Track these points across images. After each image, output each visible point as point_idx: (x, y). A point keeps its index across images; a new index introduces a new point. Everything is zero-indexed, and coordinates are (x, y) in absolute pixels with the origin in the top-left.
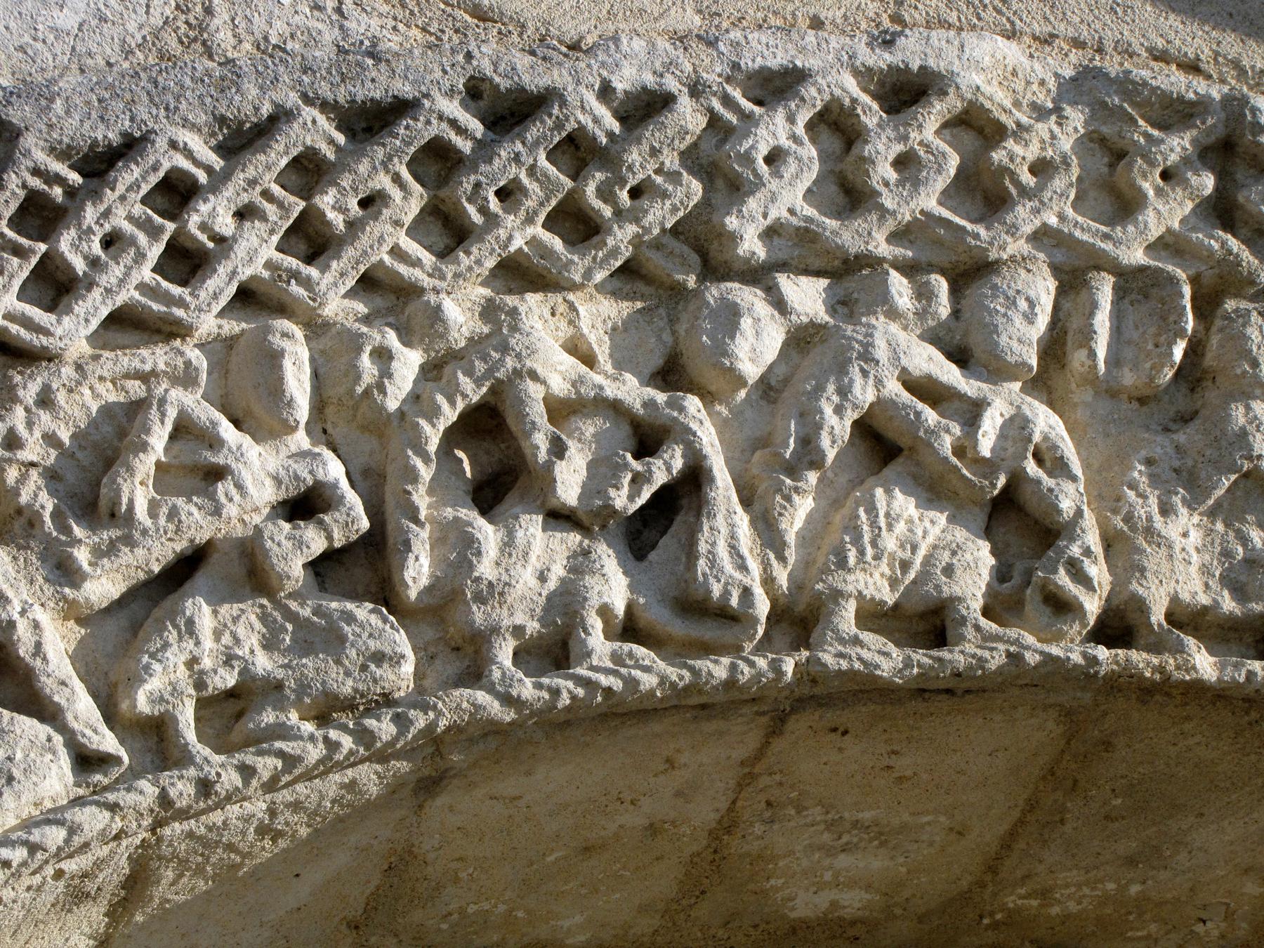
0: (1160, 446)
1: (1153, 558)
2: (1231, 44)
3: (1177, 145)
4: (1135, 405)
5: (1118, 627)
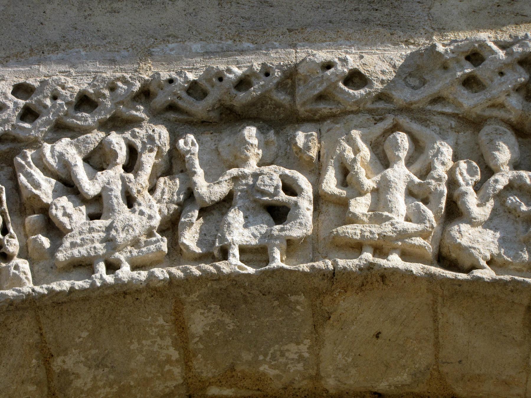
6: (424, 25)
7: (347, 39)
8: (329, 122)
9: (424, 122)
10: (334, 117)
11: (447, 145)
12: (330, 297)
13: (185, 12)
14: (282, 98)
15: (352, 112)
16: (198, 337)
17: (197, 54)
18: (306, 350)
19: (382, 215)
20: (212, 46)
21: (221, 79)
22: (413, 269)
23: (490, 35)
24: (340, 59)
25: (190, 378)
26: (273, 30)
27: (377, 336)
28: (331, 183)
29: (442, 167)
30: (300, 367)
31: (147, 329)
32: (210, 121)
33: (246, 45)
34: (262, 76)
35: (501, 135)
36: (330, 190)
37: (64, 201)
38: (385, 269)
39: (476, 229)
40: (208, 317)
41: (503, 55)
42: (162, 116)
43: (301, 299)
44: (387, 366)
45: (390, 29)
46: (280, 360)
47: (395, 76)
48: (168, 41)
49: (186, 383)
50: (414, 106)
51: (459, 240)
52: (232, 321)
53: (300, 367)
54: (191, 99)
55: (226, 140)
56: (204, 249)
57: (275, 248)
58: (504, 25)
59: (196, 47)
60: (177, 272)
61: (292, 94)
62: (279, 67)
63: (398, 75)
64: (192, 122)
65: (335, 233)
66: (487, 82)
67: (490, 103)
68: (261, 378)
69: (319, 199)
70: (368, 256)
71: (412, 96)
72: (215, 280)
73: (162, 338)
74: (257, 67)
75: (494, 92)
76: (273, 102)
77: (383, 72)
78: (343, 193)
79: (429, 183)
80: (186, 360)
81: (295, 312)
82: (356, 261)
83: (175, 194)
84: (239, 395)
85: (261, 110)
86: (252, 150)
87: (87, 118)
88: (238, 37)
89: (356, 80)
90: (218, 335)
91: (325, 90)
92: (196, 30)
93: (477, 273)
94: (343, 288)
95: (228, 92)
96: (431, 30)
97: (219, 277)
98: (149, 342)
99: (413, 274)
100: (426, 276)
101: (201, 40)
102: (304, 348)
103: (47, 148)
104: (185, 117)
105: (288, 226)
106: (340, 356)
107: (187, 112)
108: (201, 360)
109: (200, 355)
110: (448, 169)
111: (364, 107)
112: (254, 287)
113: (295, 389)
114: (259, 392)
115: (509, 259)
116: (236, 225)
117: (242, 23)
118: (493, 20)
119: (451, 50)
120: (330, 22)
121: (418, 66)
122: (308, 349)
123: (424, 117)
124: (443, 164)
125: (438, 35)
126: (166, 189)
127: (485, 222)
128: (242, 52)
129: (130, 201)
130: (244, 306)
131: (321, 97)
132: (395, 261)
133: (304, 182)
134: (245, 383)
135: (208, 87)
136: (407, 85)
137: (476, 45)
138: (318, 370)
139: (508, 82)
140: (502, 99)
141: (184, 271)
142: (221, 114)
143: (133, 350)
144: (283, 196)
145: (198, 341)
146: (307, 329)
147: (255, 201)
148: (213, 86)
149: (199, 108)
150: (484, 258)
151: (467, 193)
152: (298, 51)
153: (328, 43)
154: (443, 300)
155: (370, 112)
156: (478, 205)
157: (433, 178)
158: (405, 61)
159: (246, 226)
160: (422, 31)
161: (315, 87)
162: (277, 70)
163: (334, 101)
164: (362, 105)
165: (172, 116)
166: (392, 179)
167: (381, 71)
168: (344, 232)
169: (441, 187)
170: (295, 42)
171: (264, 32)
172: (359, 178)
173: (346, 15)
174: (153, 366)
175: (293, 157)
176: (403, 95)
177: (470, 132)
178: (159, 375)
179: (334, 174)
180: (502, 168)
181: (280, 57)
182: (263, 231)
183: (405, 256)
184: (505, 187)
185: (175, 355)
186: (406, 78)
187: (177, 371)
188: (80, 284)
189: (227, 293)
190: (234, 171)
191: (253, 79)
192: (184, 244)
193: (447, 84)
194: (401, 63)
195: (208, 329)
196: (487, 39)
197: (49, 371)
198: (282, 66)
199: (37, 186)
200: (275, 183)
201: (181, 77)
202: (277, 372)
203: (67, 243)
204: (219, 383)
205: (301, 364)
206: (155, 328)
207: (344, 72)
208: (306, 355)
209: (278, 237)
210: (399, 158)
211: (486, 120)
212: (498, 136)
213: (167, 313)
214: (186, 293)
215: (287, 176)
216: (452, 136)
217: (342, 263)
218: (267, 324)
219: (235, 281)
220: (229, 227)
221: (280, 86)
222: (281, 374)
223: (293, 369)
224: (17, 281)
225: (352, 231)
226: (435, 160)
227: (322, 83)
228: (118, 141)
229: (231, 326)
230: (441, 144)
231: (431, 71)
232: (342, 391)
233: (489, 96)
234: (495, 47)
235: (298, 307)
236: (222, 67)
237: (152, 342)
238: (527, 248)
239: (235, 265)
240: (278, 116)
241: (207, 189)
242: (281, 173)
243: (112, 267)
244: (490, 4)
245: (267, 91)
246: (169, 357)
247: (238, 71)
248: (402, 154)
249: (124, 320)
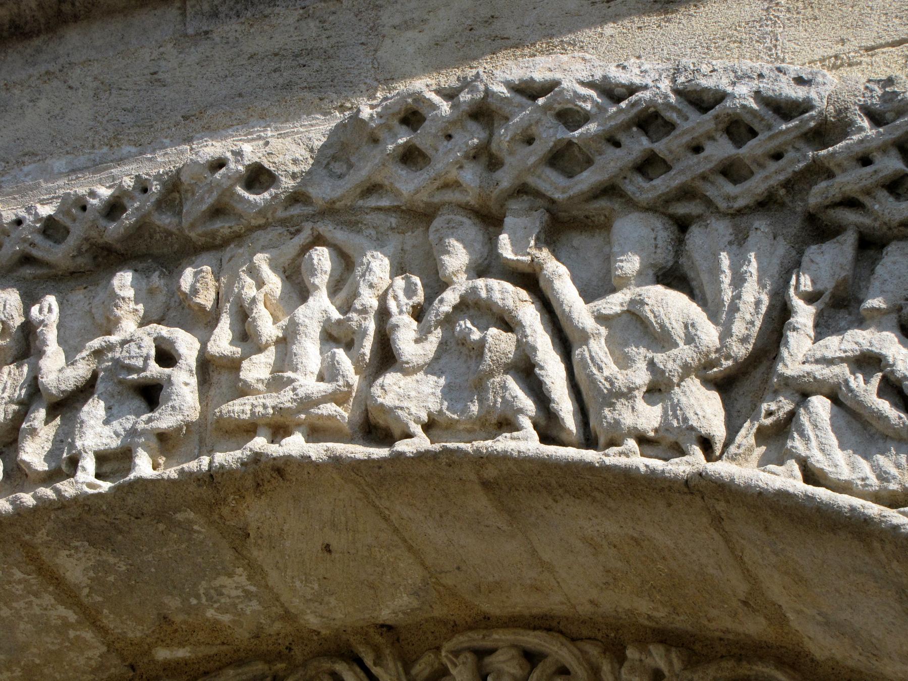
6: (366, 77)
7: (262, 117)
8: (232, 246)
9: (354, 226)
10: (237, 238)
11: (380, 255)
13: (49, 116)
14: (167, 221)
15: (260, 227)
17: (60, 175)
19: (282, 377)
20: (82, 160)
21: (84, 208)
22: (311, 454)
23: (429, 81)
24: (233, 152)
26: (162, 122)
28: (222, 341)
29: (370, 291)
30: (255, 605)
31: (7, 587)
33: (126, 149)
34: (137, 194)
35: (452, 229)
36: (218, 350)
38: (274, 459)
39: (415, 377)
41: (448, 109)
42: (15, 274)
44: (372, 586)
45: (320, 92)
47: (313, 165)
48: (23, 162)
50: (338, 205)
51: (380, 400)
53: (255, 605)
54: (48, 243)
56: (53, 464)
57: (140, 450)
58: (475, 59)
59: (59, 164)
60: (28, 499)
62: (158, 177)
63: (317, 162)
64: (56, 276)
65: (218, 414)
66: (430, 152)
67: (437, 184)
68: (215, 628)
69: (207, 367)
70: (259, 443)
71: (333, 190)
72: (59, 509)
74: (128, 182)
75: (439, 166)
77: (295, 161)
78: (237, 351)
79: (349, 319)
81: (196, 535)
82: (238, 453)
83: (18, 388)
84: (200, 655)
86: (125, 307)
88: (115, 140)
89: (264, 178)
91: (218, 201)
92: (61, 139)
93: (403, 446)
95: (94, 225)
96: (376, 83)
97: (62, 504)
99: (312, 462)
100: (330, 461)
101: (68, 153)
104: (44, 271)
105: (156, 414)
108: (112, 616)
109: (105, 611)
110: (380, 293)
111: (273, 217)
112: (117, 509)
113: (270, 635)
114: (225, 648)
115: (455, 417)
116: (92, 422)
117: (121, 120)
118: (461, 53)
119: (378, 114)
120: (240, 95)
121: (343, 143)
122: (248, 579)
123: (354, 218)
124: (371, 286)
125: (384, 89)
126: (9, 385)
127: (429, 365)
130: (120, 537)
131: (218, 211)
132: (295, 445)
134: (199, 637)
135: (67, 222)
136: (331, 174)
137: (410, 100)
138: (282, 605)
139: (457, 148)
140: (454, 174)
141: (12, 503)
142: (95, 258)
144: (154, 369)
146: (228, 555)
147: (121, 382)
148: (74, 220)
149: (58, 254)
150: (417, 421)
151: (398, 326)
152: (194, 146)
153: (235, 128)
154: (373, 489)
156: (417, 341)
157: (356, 311)
158: (328, 138)
159: (106, 422)
160: (363, 87)
161: (202, 199)
162: (155, 183)
164: (269, 215)
166: (301, 321)
167: (292, 160)
168: (229, 412)
169: (367, 322)
170: (191, 135)
171: (152, 126)
172: (256, 326)
173: (261, 82)
174: (51, 634)
176: (324, 191)
177: (421, 229)
179: (228, 326)
180: (455, 279)
181: (159, 164)
182: (128, 426)
183: (315, 433)
184: (455, 308)
186: (328, 164)
190: (97, 343)
191: (125, 201)
192: (24, 462)
193: (376, 164)
194: (321, 143)
196: (424, 89)
198: (162, 175)
200: (145, 351)
201: (30, 214)
207: (237, 171)
208: (253, 589)
209: (144, 432)
210: (316, 288)
211: (439, 209)
212: (450, 232)
214: (28, 533)
215: (163, 338)
216: (395, 241)
217: (220, 458)
219: (87, 505)
220: (81, 427)
221: (163, 205)
225: (240, 408)
226: (361, 283)
227: (210, 191)
230: (373, 256)
231: (357, 149)
232: (337, 630)
233: (432, 174)
234: (436, 99)
235: (196, 527)
236: (82, 191)
238: (478, 395)
239: (83, 483)
242: (155, 335)
244: (460, 29)
245: (144, 216)
246: (64, 619)
247: (105, 192)
248: (319, 280)
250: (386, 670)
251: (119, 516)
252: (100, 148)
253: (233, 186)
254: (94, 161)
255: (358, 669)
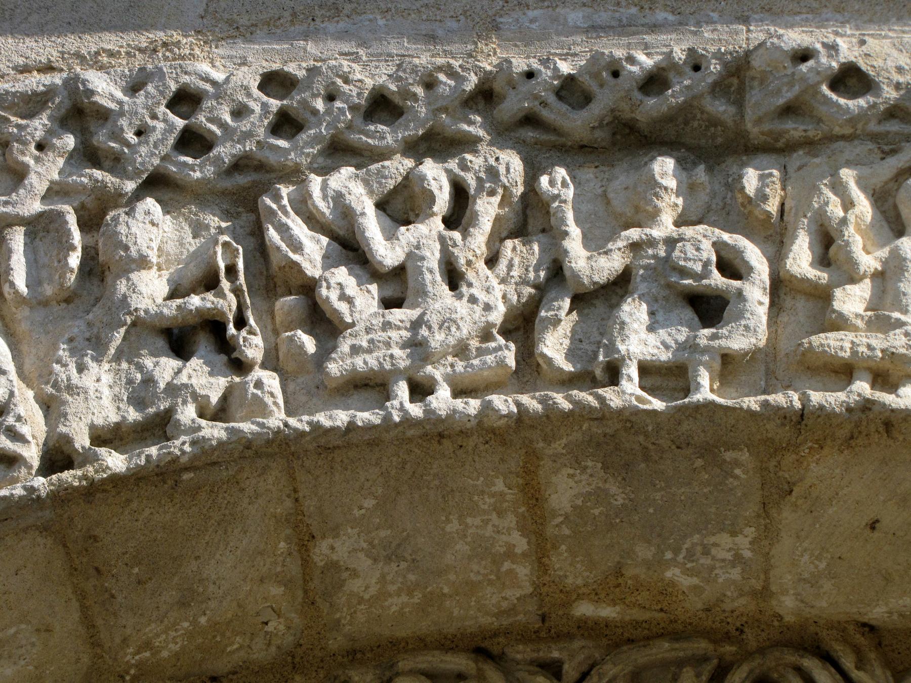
0: (77, 328)
1: (74, 405)
2: (72, 43)
3: (39, 125)
4: (64, 305)
5: (58, 457)
8: (801, 152)
10: (810, 145)
12: (794, 456)
15: (843, 137)
16: (561, 515)
17: (576, 30)
18: (748, 546)
19: (889, 317)
20: (603, 17)
21: (616, 74)
24: (824, 45)
25: (545, 584)
27: (873, 526)
28: (801, 259)
30: (735, 574)
31: (476, 498)
32: (596, 146)
33: (661, 15)
36: (799, 270)
37: (341, 274)
38: (893, 411)
40: (581, 481)
42: (512, 134)
43: (743, 458)
44: (888, 579)
46: (701, 561)
49: (537, 593)
52: (621, 490)
53: (735, 574)
54: (564, 107)
55: (621, 179)
56: (579, 366)
59: (575, 16)
61: (739, 103)
62: (718, 55)
64: (563, 146)
65: (806, 345)
68: (667, 590)
69: (781, 286)
70: (862, 387)
72: (596, 419)
73: (500, 514)
74: (679, 54)
76: (705, 116)
77: (900, 70)
80: (540, 553)
81: (731, 480)
82: (841, 396)
83: (531, 269)
84: (627, 618)
85: (683, 129)
86: (666, 198)
87: (384, 134)
89: (852, 82)
90: (597, 514)
91: (797, 98)
94: (817, 442)
95: (628, 97)
97: (604, 414)
98: (477, 521)
102: (743, 542)
103: (315, 182)
104: (553, 138)
105: (724, 331)
106: (806, 557)
107: (555, 130)
108: (565, 555)
109: (563, 547)
113: (724, 611)
114: (662, 615)
116: (635, 326)
126: (517, 261)
128: (654, 28)
129: (454, 278)
130: (643, 465)
131: (789, 110)
133: (754, 255)
134: (639, 598)
135: (593, 86)
138: (767, 580)
141: (543, 401)
142: (614, 134)
143: (450, 533)
144: (717, 279)
145: (561, 523)
146: (751, 509)
147: (669, 286)
148: (601, 86)
149: (578, 123)
152: (752, 28)
153: (804, 16)
155: (874, 137)
159: (651, 329)
161: (779, 91)
162: (714, 61)
163: (812, 117)
164: (860, 126)
165: (530, 134)
167: (896, 67)
168: (822, 345)
170: (746, 14)
172: (850, 252)
174: (484, 563)
175: (737, 213)
178: (493, 577)
179: (807, 245)
181: (721, 40)
182: (682, 338)
185: (521, 544)
187: (523, 571)
188: (365, 417)
189: (616, 441)
190: (634, 234)
191: (671, 76)
192: (544, 356)
195: (579, 502)
197: (306, 562)
198: (723, 54)
199: (297, 247)
200: (705, 256)
201: (548, 68)
202: (695, 581)
203: (345, 346)
204: (595, 597)
205: (738, 570)
206: (489, 498)
207: (830, 67)
208: (747, 554)
209: (707, 350)
213: (510, 472)
214: (544, 440)
215: (725, 244)
217: (816, 397)
218: (683, 498)
219: (630, 421)
220: (622, 329)
221: (718, 89)
222: (701, 584)
223: (723, 577)
224: (260, 408)
225: (836, 343)
227: (791, 85)
228: (435, 175)
229: (619, 498)
232: (807, 619)
235: (737, 471)
236: (619, 53)
237: (483, 521)
239: (631, 395)
240: (713, 140)
241: (588, 263)
242: (715, 239)
243: (421, 390)
245: (694, 98)
246: (511, 547)
247: (646, 61)
249: (437, 482)
250: (873, 676)
251: (661, 442)
252: (628, 6)
253: (820, 83)
254: (620, 21)
255: (833, 670)
